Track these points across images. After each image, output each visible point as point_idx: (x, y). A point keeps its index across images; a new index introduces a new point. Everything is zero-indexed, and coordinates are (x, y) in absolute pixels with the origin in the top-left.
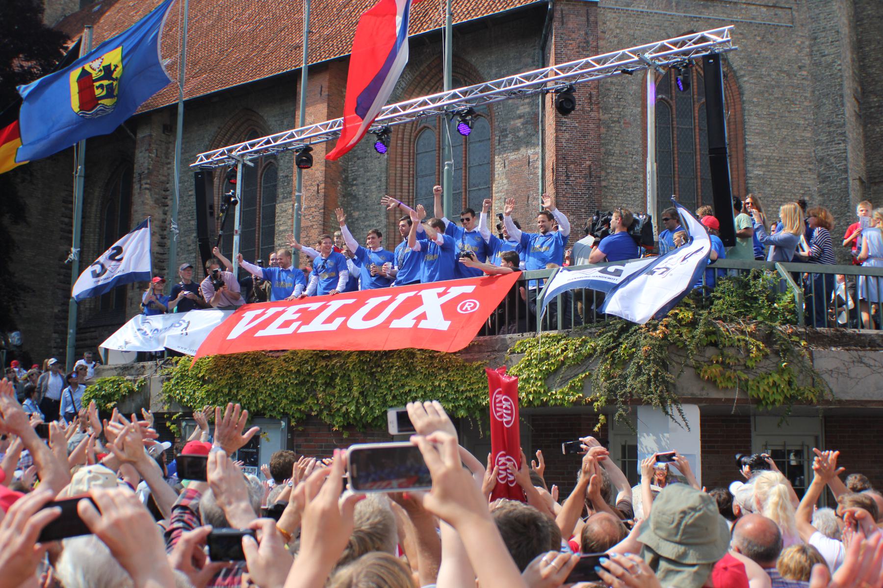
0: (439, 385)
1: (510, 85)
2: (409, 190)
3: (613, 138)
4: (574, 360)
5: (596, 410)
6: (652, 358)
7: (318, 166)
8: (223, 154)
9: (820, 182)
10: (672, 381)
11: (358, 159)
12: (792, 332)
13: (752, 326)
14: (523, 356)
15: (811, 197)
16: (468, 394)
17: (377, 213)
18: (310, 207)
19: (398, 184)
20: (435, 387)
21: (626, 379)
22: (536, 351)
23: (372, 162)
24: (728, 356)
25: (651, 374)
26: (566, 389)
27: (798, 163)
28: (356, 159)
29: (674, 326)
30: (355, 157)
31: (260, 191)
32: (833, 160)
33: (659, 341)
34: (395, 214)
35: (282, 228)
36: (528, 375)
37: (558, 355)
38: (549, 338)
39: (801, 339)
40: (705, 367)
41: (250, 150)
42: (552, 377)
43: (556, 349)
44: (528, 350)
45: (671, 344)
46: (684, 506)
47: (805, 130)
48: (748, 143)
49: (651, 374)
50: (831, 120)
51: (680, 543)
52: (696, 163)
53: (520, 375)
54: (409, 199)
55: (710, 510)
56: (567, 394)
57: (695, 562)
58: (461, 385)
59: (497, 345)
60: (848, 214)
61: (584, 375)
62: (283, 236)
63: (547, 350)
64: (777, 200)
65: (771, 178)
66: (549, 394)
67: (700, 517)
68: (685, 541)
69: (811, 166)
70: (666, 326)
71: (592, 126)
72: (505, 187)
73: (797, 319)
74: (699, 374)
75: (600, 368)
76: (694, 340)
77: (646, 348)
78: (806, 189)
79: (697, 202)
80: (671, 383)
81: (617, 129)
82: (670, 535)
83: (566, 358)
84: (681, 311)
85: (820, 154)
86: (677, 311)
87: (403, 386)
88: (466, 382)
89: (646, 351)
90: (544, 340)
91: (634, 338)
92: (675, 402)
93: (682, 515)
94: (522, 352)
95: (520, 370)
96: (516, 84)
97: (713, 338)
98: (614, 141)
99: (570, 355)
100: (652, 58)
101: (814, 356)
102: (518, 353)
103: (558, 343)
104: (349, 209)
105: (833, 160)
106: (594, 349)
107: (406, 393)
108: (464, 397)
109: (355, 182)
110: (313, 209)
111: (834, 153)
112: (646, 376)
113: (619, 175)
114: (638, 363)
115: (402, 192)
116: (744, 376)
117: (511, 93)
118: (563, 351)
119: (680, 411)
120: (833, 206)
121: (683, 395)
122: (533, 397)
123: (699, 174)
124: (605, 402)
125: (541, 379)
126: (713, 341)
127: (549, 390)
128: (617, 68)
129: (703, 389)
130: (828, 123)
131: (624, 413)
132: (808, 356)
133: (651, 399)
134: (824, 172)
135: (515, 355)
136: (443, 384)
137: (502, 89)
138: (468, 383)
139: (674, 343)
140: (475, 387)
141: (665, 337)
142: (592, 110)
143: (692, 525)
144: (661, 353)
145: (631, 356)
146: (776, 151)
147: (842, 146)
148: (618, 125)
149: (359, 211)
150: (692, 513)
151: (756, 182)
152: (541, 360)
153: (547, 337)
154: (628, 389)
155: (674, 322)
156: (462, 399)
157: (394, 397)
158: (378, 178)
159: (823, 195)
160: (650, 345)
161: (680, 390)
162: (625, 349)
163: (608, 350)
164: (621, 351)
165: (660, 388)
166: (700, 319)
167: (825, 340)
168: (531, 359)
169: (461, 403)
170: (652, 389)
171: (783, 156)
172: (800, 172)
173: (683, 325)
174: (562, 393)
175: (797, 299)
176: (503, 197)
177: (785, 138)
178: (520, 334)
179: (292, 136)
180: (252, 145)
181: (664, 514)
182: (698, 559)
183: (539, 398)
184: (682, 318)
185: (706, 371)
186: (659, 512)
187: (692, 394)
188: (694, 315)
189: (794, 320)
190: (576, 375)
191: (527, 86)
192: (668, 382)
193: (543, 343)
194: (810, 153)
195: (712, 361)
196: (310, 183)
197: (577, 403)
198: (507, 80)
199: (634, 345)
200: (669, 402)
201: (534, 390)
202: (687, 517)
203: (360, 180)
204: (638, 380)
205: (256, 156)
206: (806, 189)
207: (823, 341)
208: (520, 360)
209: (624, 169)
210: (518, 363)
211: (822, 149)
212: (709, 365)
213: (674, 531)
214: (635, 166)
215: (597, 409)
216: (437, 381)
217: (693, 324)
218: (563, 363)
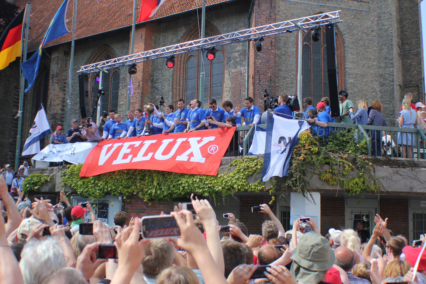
0: (196, 181)
1: (233, 36)
2: (183, 85)
3: (282, 63)
4: (260, 170)
5: (270, 194)
8: (93, 66)
9: (380, 86)
10: (307, 181)
11: (159, 70)
12: (365, 158)
13: (346, 155)
14: (236, 168)
15: (376, 93)
16: (209, 185)
17: (167, 96)
18: (135, 93)
19: (178, 83)
20: (194, 181)
22: (242, 165)
23: (165, 72)
24: (334, 169)
25: (298, 177)
26: (256, 184)
27: (370, 77)
28: (158, 70)
30: (157, 69)
31: (111, 85)
32: (387, 75)
34: (176, 97)
35: (121, 103)
36: (239, 176)
37: (253, 167)
38: (249, 159)
39: (369, 162)
40: (324, 174)
41: (106, 65)
42: (250, 178)
43: (252, 164)
44: (239, 165)
45: (307, 163)
46: (313, 243)
47: (374, 61)
48: (346, 66)
49: (298, 177)
50: (386, 57)
51: (310, 260)
52: (322, 75)
53: (234, 176)
54: (183, 90)
55: (326, 246)
56: (257, 186)
57: (317, 270)
58: (206, 181)
59: (224, 162)
60: (394, 102)
62: (122, 107)
63: (248, 165)
64: (360, 94)
65: (357, 84)
66: (248, 186)
67: (320, 249)
68: (313, 260)
69: (376, 79)
70: (305, 154)
71: (272, 57)
73: (368, 152)
74: (320, 178)
77: (294, 165)
78: (374, 89)
79: (322, 95)
80: (307, 182)
81: (284, 58)
82: (306, 256)
83: (257, 169)
84: (312, 147)
85: (381, 73)
86: (310, 147)
87: (178, 181)
88: (208, 179)
89: (295, 166)
90: (246, 160)
92: (309, 191)
93: (312, 247)
94: (236, 165)
95: (235, 174)
96: (235, 36)
97: (328, 161)
98: (282, 64)
99: (259, 167)
100: (301, 25)
101: (375, 170)
103: (253, 161)
104: (154, 94)
105: (387, 75)
107: (179, 184)
108: (207, 186)
109: (157, 81)
110: (137, 94)
111: (387, 72)
113: (284, 81)
114: (291, 172)
116: (342, 179)
117: (233, 40)
118: (255, 165)
119: (311, 195)
120: (386, 98)
121: (313, 187)
122: (241, 187)
123: (323, 81)
124: (275, 190)
126: (328, 162)
127: (248, 184)
129: (322, 185)
130: (385, 58)
131: (284, 196)
132: (372, 170)
133: (297, 189)
134: (383, 81)
135: (232, 167)
136: (198, 180)
137: (229, 38)
138: (209, 180)
139: (309, 163)
140: (213, 182)
141: (304, 160)
142: (272, 49)
143: (317, 252)
144: (303, 167)
146: (360, 71)
147: (392, 69)
148: (284, 56)
149: (159, 95)
150: (317, 247)
151: (350, 85)
152: (245, 170)
154: (287, 185)
155: (309, 152)
156: (206, 188)
157: (174, 186)
158: (168, 80)
159: (382, 92)
160: (297, 163)
161: (311, 185)
165: (302, 184)
166: (321, 151)
167: (381, 162)
169: (206, 190)
170: (298, 184)
171: (363, 73)
172: (371, 81)
173: (313, 154)
174: (255, 185)
175: (368, 143)
176: (228, 90)
177: (364, 65)
178: (235, 157)
179: (127, 59)
180: (107, 63)
181: (303, 246)
182: (318, 269)
183: (243, 187)
184: (313, 151)
185: (324, 176)
186: (301, 245)
187: (317, 187)
189: (366, 152)
192: (305, 181)
193: (246, 161)
194: (376, 72)
195: (327, 172)
196: (135, 81)
197: (261, 190)
198: (231, 34)
200: (306, 191)
201: (241, 184)
202: (314, 248)
203: (159, 81)
205: (109, 68)
206: (374, 89)
207: (380, 163)
208: (235, 169)
209: (287, 78)
210: (233, 171)
211: (382, 71)
212: (325, 174)
213: (308, 255)
214: (292, 77)
215: (271, 193)
216: (195, 178)
217: (318, 153)
218: (255, 171)
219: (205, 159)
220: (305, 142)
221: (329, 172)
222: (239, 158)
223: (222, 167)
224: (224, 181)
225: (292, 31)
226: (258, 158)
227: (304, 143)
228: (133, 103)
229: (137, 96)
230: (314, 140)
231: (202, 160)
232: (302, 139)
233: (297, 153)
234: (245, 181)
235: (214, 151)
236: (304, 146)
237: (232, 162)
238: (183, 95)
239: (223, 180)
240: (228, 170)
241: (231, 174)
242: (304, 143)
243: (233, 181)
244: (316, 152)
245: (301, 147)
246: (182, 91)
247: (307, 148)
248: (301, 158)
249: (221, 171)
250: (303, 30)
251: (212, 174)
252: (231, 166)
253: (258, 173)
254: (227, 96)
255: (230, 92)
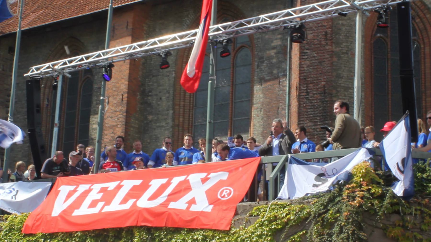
0: (197, 238)
1: (258, 22)
2: (190, 100)
6: (350, 221)
7: (123, 81)
8: (49, 67)
10: (365, 238)
11: (153, 76)
13: (427, 200)
14: (258, 218)
17: (166, 117)
18: (116, 111)
21: (332, 236)
22: (267, 215)
25: (349, 233)
29: (368, 199)
33: (356, 208)
34: (179, 118)
36: (262, 232)
37: (283, 218)
38: (278, 205)
40: (391, 229)
43: (281, 214)
44: (262, 214)
53: (255, 232)
54: (190, 107)
61: (301, 233)
70: (362, 198)
71: (327, 56)
72: (261, 100)
74: (386, 234)
75: (314, 229)
76: (383, 209)
77: (345, 214)
80: (364, 240)
81: (345, 58)
83: (289, 220)
84: (373, 187)
86: (370, 187)
88: (216, 236)
89: (347, 216)
90: (273, 207)
91: (338, 206)
94: (258, 215)
95: (256, 228)
96: (262, 21)
97: (396, 208)
98: (343, 68)
99: (292, 218)
100: (360, 5)
102: (255, 216)
103: (284, 209)
106: (309, 214)
109: (150, 94)
110: (118, 113)
112: (346, 234)
113: (346, 93)
114: (341, 224)
115: (184, 102)
116: (419, 236)
117: (258, 28)
118: (287, 215)
125: (270, 235)
126: (397, 210)
128: (336, 10)
135: (252, 217)
136: (200, 237)
138: (217, 237)
141: (361, 206)
142: (327, 44)
144: (357, 217)
145: (336, 219)
148: (346, 55)
153: (276, 205)
155: (368, 195)
160: (349, 211)
162: (331, 214)
163: (320, 215)
164: (328, 215)
166: (387, 193)
168: (264, 221)
173: (374, 198)
176: (260, 107)
179: (99, 56)
180: (71, 62)
184: (374, 193)
185: (391, 232)
188: (382, 191)
190: (296, 233)
191: (272, 24)
192: (362, 239)
193: (273, 209)
195: (395, 225)
196: (116, 93)
198: (256, 19)
199: (338, 211)
204: (340, 237)
205: (73, 70)
208: (256, 221)
212: (393, 228)
216: (195, 235)
217: (382, 197)
218: (287, 223)
219: (211, 206)
220: (362, 179)
221: (399, 225)
222: (262, 204)
223: (236, 218)
224: (239, 239)
225: (346, 14)
226: (291, 204)
227: (360, 181)
228: (113, 126)
229: (119, 116)
230: (376, 176)
231: (209, 209)
232: (358, 175)
233: (350, 196)
234: (270, 240)
235: (226, 196)
236: (361, 186)
237: (252, 210)
238: (189, 114)
239: (238, 238)
240: (247, 222)
241: (251, 228)
242: (360, 181)
243: (253, 238)
244: (379, 194)
245: (356, 187)
246: (188, 108)
247: (365, 188)
248: (356, 203)
249: (236, 223)
250: (363, 12)
251: (222, 228)
252: (251, 216)
253: (292, 226)
254: (258, 116)
255: (262, 110)
